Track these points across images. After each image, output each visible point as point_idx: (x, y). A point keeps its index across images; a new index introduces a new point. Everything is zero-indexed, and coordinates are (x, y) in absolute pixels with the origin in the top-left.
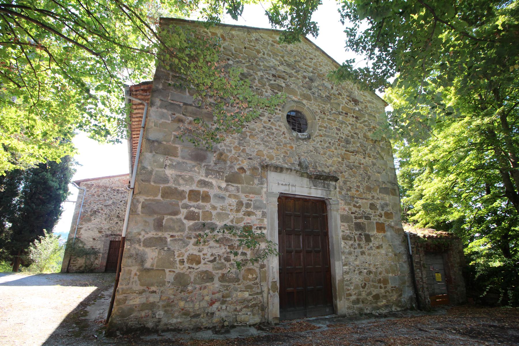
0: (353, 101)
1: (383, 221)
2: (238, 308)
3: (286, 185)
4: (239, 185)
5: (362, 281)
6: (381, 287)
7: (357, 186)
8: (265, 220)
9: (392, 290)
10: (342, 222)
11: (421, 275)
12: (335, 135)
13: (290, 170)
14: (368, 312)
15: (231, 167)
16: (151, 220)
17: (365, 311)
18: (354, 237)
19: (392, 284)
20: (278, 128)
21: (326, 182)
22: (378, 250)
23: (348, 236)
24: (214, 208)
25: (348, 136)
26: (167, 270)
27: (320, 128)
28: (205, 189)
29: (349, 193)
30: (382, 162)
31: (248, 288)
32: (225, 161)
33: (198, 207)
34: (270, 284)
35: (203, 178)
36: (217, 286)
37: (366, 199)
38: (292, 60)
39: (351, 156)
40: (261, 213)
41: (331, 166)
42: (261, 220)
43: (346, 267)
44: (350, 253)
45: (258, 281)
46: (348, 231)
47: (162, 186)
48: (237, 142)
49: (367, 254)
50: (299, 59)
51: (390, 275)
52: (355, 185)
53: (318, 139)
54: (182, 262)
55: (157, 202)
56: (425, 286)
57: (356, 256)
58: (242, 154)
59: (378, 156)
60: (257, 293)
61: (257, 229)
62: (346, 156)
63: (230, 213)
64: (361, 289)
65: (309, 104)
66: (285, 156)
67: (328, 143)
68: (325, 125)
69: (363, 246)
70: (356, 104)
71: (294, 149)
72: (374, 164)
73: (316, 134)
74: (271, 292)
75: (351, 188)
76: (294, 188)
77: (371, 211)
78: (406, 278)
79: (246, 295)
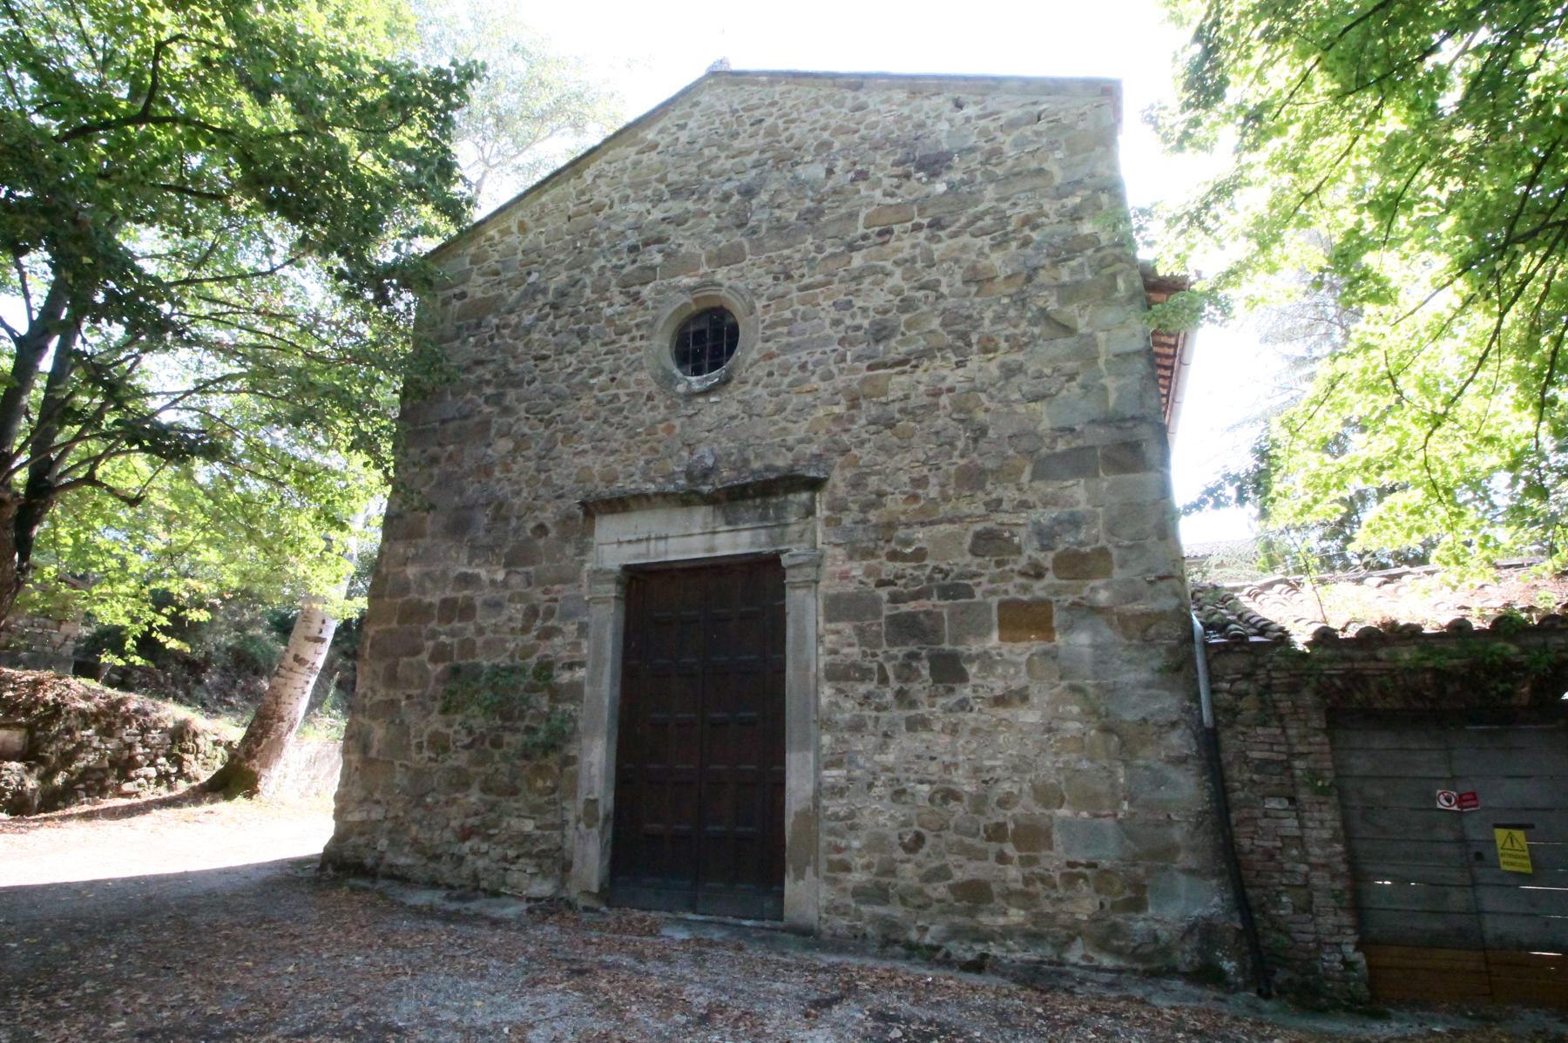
0: (920, 168)
1: (1041, 594)
2: (511, 853)
3: (639, 541)
4: (531, 569)
5: (906, 824)
6: (1002, 858)
7: (913, 480)
8: (585, 644)
9: (1070, 880)
10: (829, 620)
11: (1272, 821)
12: (828, 331)
13: (644, 501)
14: (927, 940)
15: (516, 531)
16: (381, 667)
17: (914, 935)
18: (881, 667)
19: (1067, 850)
20: (634, 389)
21: (774, 500)
22: (1003, 713)
23: (854, 665)
24: (480, 631)
25: (886, 312)
26: (397, 763)
27: (768, 333)
28: (467, 592)
29: (873, 516)
30: (1063, 345)
31: (535, 811)
32: (506, 519)
33: (452, 634)
34: (581, 806)
35: (464, 570)
36: (473, 799)
37: (951, 521)
38: (692, 167)
39: (896, 379)
40: (575, 627)
41: (801, 441)
42: (576, 646)
43: (834, 772)
44: (857, 726)
45: (557, 795)
46: (856, 650)
47: (399, 601)
48: (532, 464)
49: (937, 727)
50: (714, 150)
51: (1064, 812)
52: (905, 479)
53: (760, 372)
54: (420, 747)
55: (391, 632)
56: (1320, 879)
57: (886, 735)
58: (542, 491)
59: (1036, 330)
60: (553, 826)
61: (563, 667)
62: (867, 390)
63: (509, 637)
64: (900, 854)
65: (734, 274)
66: (648, 462)
67: (795, 368)
68: (788, 314)
69: (923, 697)
70: (934, 175)
71: (677, 430)
72: (1009, 372)
73: (755, 355)
74: (582, 826)
75: (881, 494)
76: (661, 545)
77: (974, 563)
78: (1177, 835)
79: (529, 826)
